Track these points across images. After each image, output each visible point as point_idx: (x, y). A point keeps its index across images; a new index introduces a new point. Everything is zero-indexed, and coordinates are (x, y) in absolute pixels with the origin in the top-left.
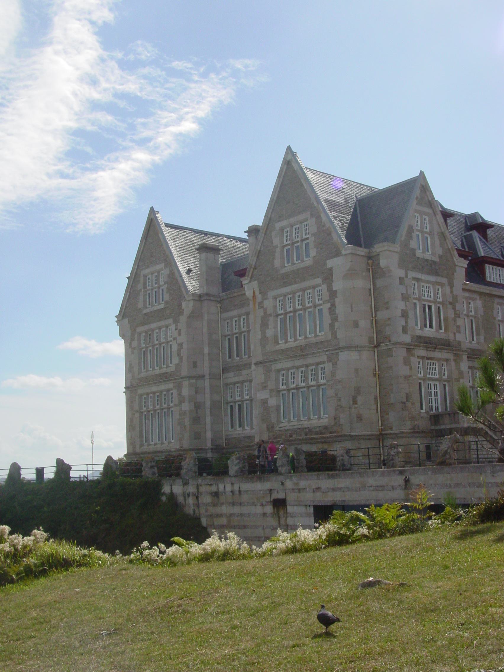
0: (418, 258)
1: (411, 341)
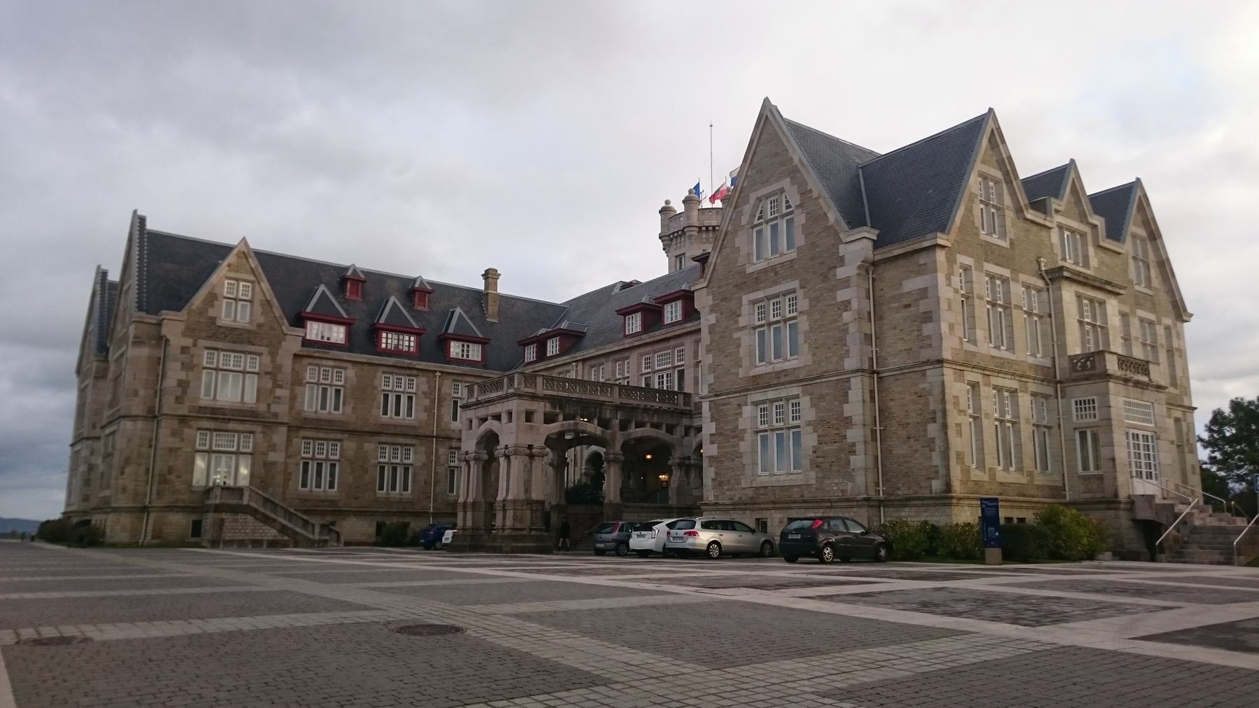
0: (220, 327)
1: (190, 412)
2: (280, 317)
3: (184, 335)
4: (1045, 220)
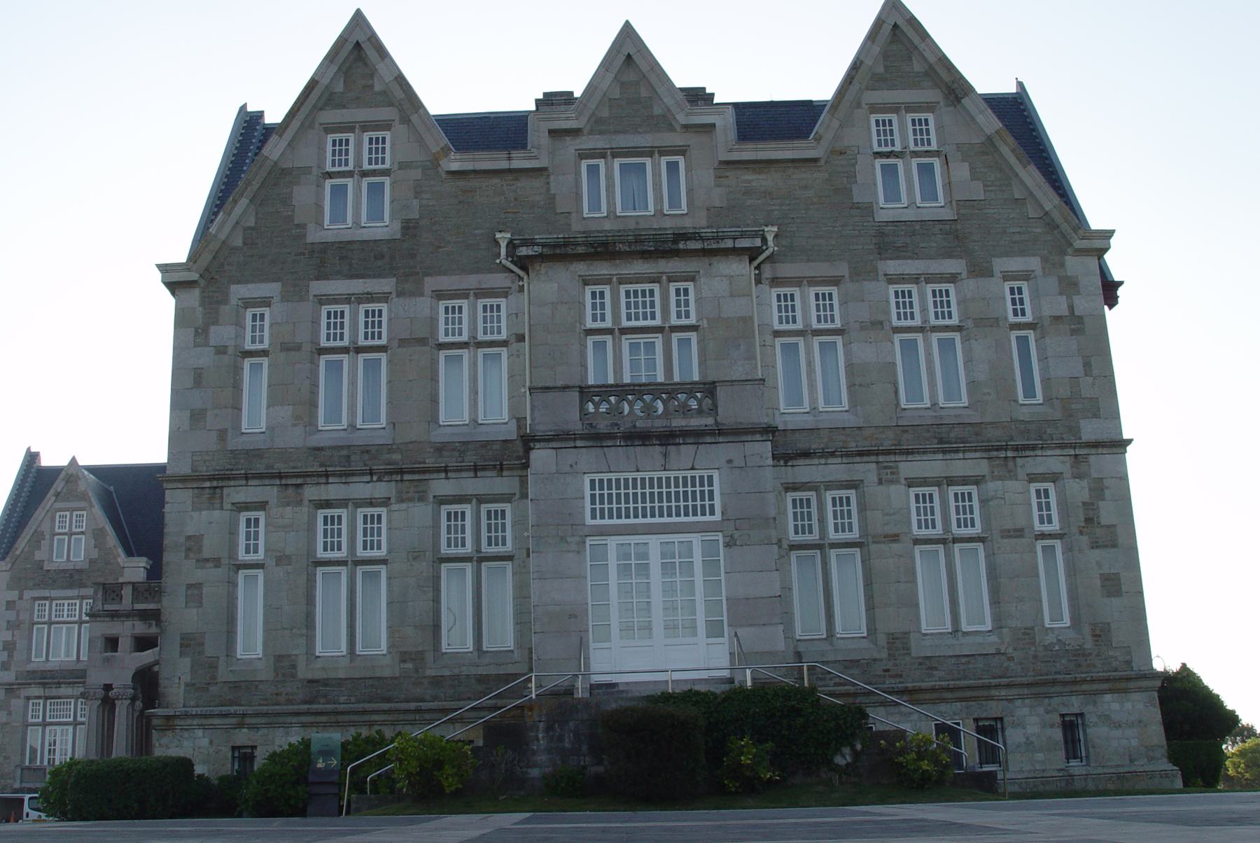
1: (16, 679)
2: (114, 546)
3: (9, 588)
4: (509, 159)
